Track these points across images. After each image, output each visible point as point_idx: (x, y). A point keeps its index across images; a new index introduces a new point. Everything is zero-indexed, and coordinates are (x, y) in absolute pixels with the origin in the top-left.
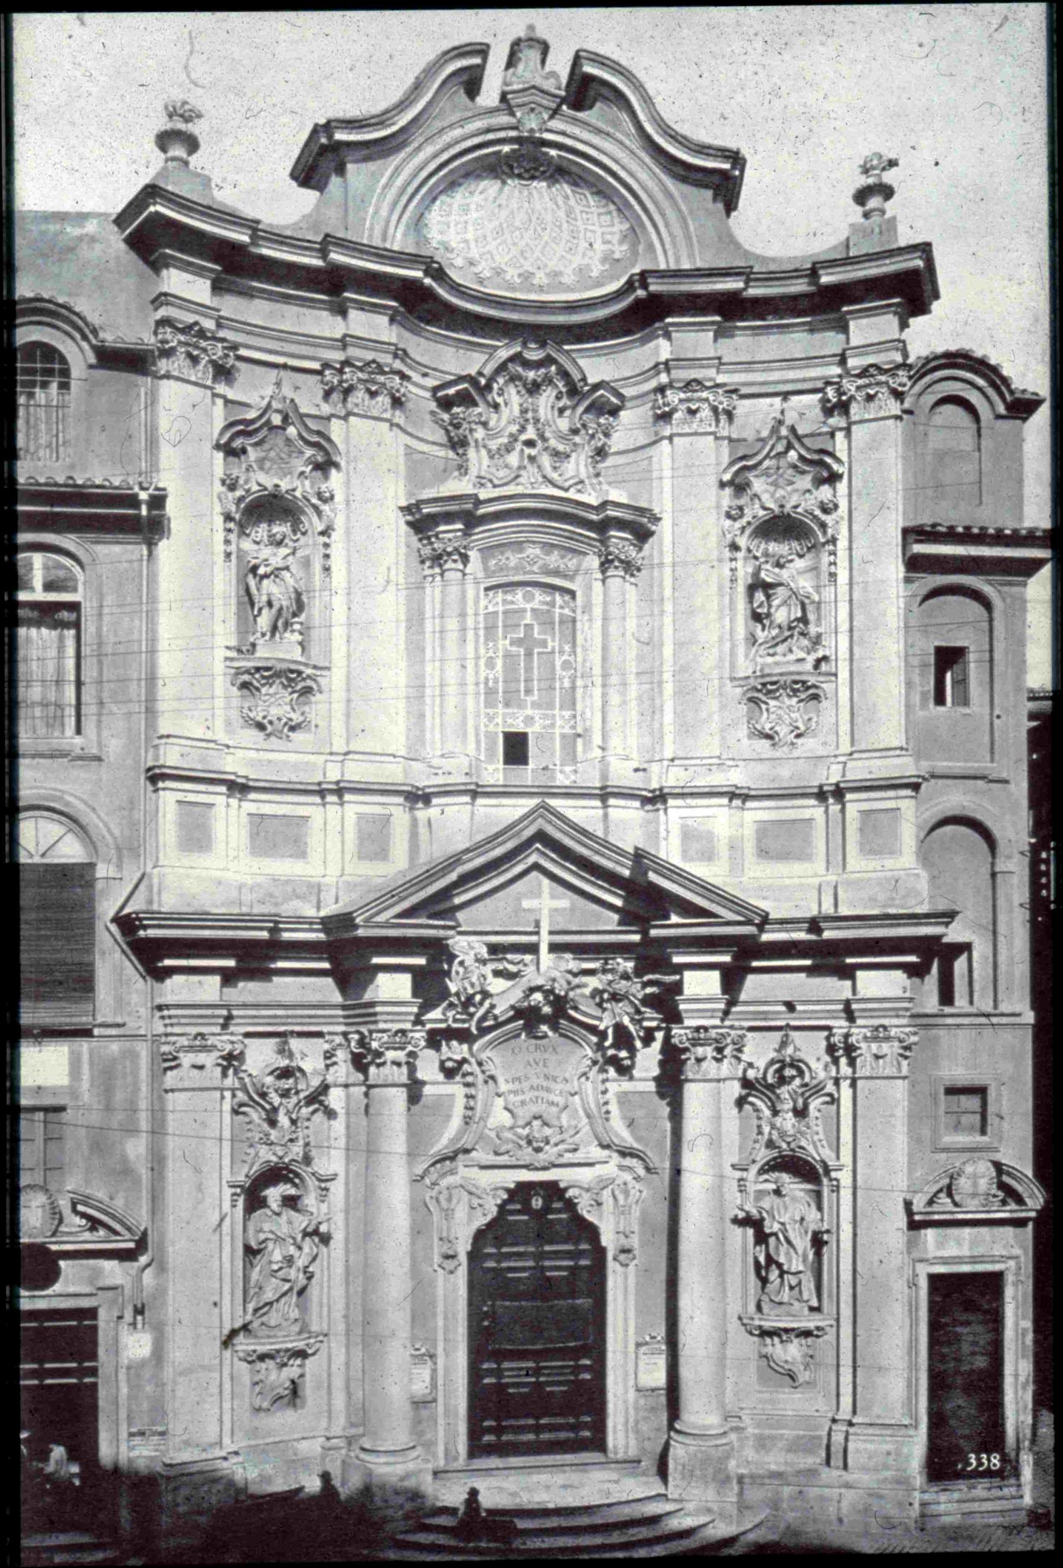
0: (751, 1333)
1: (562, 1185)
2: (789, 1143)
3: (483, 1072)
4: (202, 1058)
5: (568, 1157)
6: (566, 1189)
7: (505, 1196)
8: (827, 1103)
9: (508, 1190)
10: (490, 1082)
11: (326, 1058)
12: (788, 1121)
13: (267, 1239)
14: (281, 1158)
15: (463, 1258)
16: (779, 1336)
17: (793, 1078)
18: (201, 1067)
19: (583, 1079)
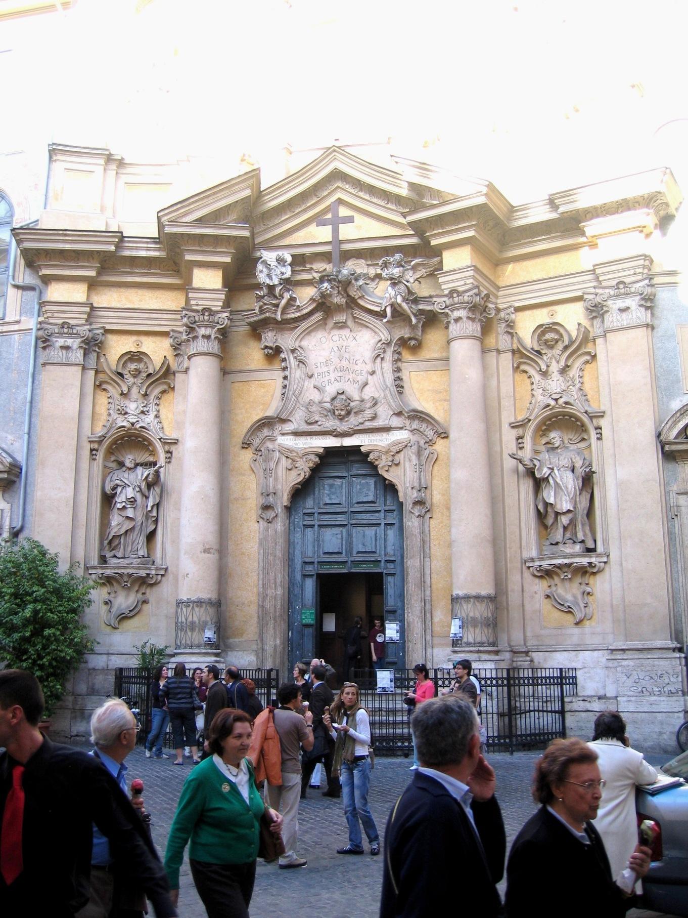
0: (535, 576)
1: (362, 449)
2: (556, 400)
3: (295, 358)
4: (69, 342)
5: (368, 425)
6: (367, 454)
7: (317, 459)
8: (587, 362)
9: (317, 455)
10: (301, 365)
11: (176, 349)
12: (555, 384)
13: (117, 485)
14: (133, 424)
15: (279, 510)
16: (558, 575)
17: (557, 341)
18: (67, 348)
19: (379, 360)
